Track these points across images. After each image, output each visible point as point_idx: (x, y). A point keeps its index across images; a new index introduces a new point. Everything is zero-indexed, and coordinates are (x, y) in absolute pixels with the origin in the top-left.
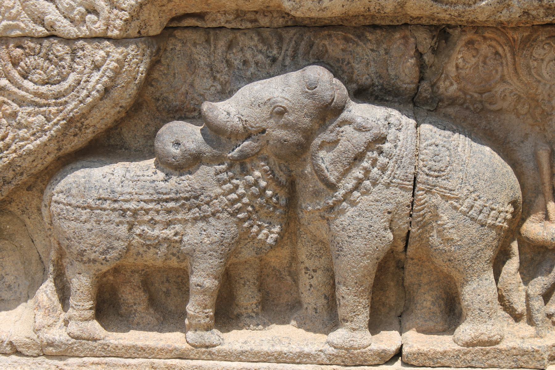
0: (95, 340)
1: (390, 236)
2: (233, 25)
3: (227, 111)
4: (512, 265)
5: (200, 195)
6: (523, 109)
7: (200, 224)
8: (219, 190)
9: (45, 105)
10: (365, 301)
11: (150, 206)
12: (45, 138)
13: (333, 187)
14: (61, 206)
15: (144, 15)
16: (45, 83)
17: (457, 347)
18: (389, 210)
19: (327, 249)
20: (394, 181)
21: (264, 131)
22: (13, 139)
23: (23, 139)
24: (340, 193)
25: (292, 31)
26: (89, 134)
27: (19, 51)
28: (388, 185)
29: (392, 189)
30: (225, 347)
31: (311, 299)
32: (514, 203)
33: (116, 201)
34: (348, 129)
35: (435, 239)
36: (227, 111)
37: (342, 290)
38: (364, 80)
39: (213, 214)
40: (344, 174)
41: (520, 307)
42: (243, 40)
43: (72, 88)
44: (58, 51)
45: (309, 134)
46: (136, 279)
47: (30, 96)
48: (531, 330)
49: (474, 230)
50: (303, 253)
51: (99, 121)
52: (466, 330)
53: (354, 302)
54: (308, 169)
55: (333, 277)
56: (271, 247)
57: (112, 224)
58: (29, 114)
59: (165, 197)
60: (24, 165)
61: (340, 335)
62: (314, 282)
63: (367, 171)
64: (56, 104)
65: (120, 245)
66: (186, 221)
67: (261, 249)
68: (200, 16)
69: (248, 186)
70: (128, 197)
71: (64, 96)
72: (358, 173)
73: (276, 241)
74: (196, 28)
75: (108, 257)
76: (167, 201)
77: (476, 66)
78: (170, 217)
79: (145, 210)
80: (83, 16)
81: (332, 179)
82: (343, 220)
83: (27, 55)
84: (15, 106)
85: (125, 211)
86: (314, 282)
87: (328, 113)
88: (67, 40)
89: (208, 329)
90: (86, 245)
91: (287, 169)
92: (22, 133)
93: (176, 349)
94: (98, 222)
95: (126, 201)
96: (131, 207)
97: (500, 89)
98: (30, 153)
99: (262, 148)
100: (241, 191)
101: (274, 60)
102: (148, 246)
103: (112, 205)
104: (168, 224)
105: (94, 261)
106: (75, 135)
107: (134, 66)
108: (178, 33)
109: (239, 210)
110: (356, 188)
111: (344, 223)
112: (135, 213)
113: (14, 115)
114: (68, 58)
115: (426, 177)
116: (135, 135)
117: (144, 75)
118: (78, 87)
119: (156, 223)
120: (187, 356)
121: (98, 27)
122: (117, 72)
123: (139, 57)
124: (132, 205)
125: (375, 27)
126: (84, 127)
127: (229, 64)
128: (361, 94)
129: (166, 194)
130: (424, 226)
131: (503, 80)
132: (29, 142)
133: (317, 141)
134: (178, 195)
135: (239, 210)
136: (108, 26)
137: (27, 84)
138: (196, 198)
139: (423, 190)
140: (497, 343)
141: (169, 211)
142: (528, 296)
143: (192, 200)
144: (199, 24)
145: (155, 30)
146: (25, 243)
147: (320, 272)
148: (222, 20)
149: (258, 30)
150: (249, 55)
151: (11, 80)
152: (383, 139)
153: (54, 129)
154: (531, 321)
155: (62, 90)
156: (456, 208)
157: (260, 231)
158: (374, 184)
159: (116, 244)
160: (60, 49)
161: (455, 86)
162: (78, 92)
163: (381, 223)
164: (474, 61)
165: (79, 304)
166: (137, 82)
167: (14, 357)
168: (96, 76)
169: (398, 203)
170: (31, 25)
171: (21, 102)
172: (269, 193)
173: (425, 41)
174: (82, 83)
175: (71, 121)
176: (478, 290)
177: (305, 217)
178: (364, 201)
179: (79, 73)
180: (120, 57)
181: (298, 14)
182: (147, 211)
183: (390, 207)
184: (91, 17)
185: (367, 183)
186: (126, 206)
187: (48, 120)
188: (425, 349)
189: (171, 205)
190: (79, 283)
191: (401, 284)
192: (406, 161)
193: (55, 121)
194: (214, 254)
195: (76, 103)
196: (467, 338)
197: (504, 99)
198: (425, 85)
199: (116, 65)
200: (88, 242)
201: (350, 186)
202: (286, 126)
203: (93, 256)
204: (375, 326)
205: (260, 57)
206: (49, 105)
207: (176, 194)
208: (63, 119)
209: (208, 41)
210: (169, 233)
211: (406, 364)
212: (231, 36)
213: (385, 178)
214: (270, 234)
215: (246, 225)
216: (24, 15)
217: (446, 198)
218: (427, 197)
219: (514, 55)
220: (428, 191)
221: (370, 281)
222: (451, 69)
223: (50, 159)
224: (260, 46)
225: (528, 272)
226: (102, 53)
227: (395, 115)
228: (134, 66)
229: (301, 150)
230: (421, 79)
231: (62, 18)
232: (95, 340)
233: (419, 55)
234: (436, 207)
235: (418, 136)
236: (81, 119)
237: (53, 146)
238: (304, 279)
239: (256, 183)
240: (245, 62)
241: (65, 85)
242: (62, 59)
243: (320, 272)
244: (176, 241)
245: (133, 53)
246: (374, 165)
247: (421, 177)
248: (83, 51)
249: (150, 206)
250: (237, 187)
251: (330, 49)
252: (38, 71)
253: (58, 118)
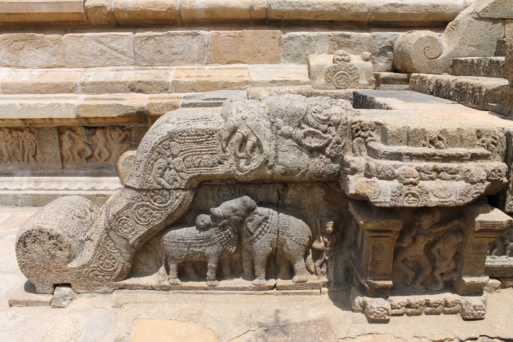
0: (178, 285)
1: (271, 249)
2: (220, 184)
3: (218, 211)
4: (310, 257)
6: (311, 207)
7: (211, 247)
8: (216, 236)
10: (264, 270)
11: (195, 241)
12: (161, 221)
13: (252, 234)
15: (192, 181)
16: (161, 203)
17: (293, 283)
19: (251, 254)
21: (230, 217)
22: (151, 221)
23: (154, 221)
24: (255, 236)
25: (238, 185)
26: (175, 219)
27: (153, 194)
28: (270, 233)
29: (271, 234)
30: (220, 286)
31: (247, 270)
32: (309, 237)
34: (256, 215)
35: (285, 249)
36: (218, 211)
37: (256, 266)
38: (261, 200)
39: (215, 243)
40: (256, 230)
41: (313, 270)
42: (223, 188)
43: (170, 205)
45: (244, 217)
46: (191, 265)
47: (156, 208)
48: (317, 277)
49: (297, 246)
50: (244, 255)
51: (178, 215)
52: (296, 278)
53: (260, 270)
54: (244, 228)
55: (253, 263)
56: (233, 253)
58: (156, 213)
61: (256, 281)
62: (247, 264)
63: (263, 228)
65: (186, 254)
66: (206, 246)
67: (230, 254)
68: (209, 181)
69: (225, 234)
72: (260, 229)
73: (235, 251)
74: (208, 185)
76: (200, 240)
77: (296, 195)
78: (201, 245)
80: (173, 182)
81: (252, 231)
82: (256, 244)
83: (156, 195)
85: (187, 243)
86: (247, 264)
87: (250, 210)
88: (168, 190)
89: (214, 280)
91: (238, 228)
92: (154, 219)
94: (178, 247)
97: (303, 201)
98: (156, 225)
99: (229, 222)
100: (223, 236)
101: (233, 194)
102: (194, 254)
104: (200, 247)
105: (177, 259)
108: (202, 187)
109: (223, 242)
110: (260, 234)
112: (190, 244)
114: (168, 195)
119: (197, 247)
121: (178, 185)
122: (183, 199)
124: (189, 241)
125: (264, 183)
127: (219, 196)
128: (261, 204)
130: (282, 245)
131: (304, 199)
133: (247, 219)
135: (223, 242)
136: (180, 185)
137: (156, 204)
138: (209, 238)
140: (306, 281)
141: (200, 243)
142: (315, 266)
143: (207, 239)
144: (209, 183)
145: (195, 186)
146: (155, 254)
147: (249, 261)
148: (216, 182)
149: (227, 185)
150: (225, 193)
151: (151, 203)
152: (268, 218)
154: (316, 274)
156: (291, 239)
158: (265, 232)
159: (184, 254)
160: (166, 193)
161: (290, 201)
163: (268, 245)
164: (295, 193)
167: (152, 291)
168: (177, 201)
169: (273, 238)
170: (157, 185)
171: (154, 209)
172: (232, 236)
173: (280, 187)
175: (169, 215)
176: (299, 265)
177: (244, 243)
178: (262, 238)
181: (240, 180)
182: (194, 243)
183: (270, 240)
185: (263, 232)
186: (187, 241)
187: (162, 215)
188: (283, 284)
189: (201, 241)
191: (275, 264)
192: (275, 225)
196: (296, 280)
197: (305, 204)
198: (280, 201)
201: (258, 233)
202: (237, 215)
203: (177, 258)
204: (267, 278)
205: (228, 193)
209: (212, 189)
210: (201, 250)
211: (277, 289)
212: (219, 187)
213: (269, 231)
214: (233, 249)
216: (155, 182)
217: (288, 236)
218: (282, 236)
219: (307, 191)
220: (282, 234)
221: (265, 263)
222: (289, 196)
223: (163, 227)
224: (228, 190)
225: (315, 259)
226: (179, 193)
227: (271, 210)
229: (241, 223)
230: (279, 199)
231: (166, 183)
232: (178, 285)
233: (278, 192)
234: (285, 239)
235: (279, 217)
237: (164, 223)
238: (244, 264)
239: (228, 233)
240: (224, 195)
241: (167, 204)
242: (166, 196)
243: (249, 261)
246: (265, 226)
247: (280, 230)
249: (195, 241)
250: (222, 235)
251: (250, 190)
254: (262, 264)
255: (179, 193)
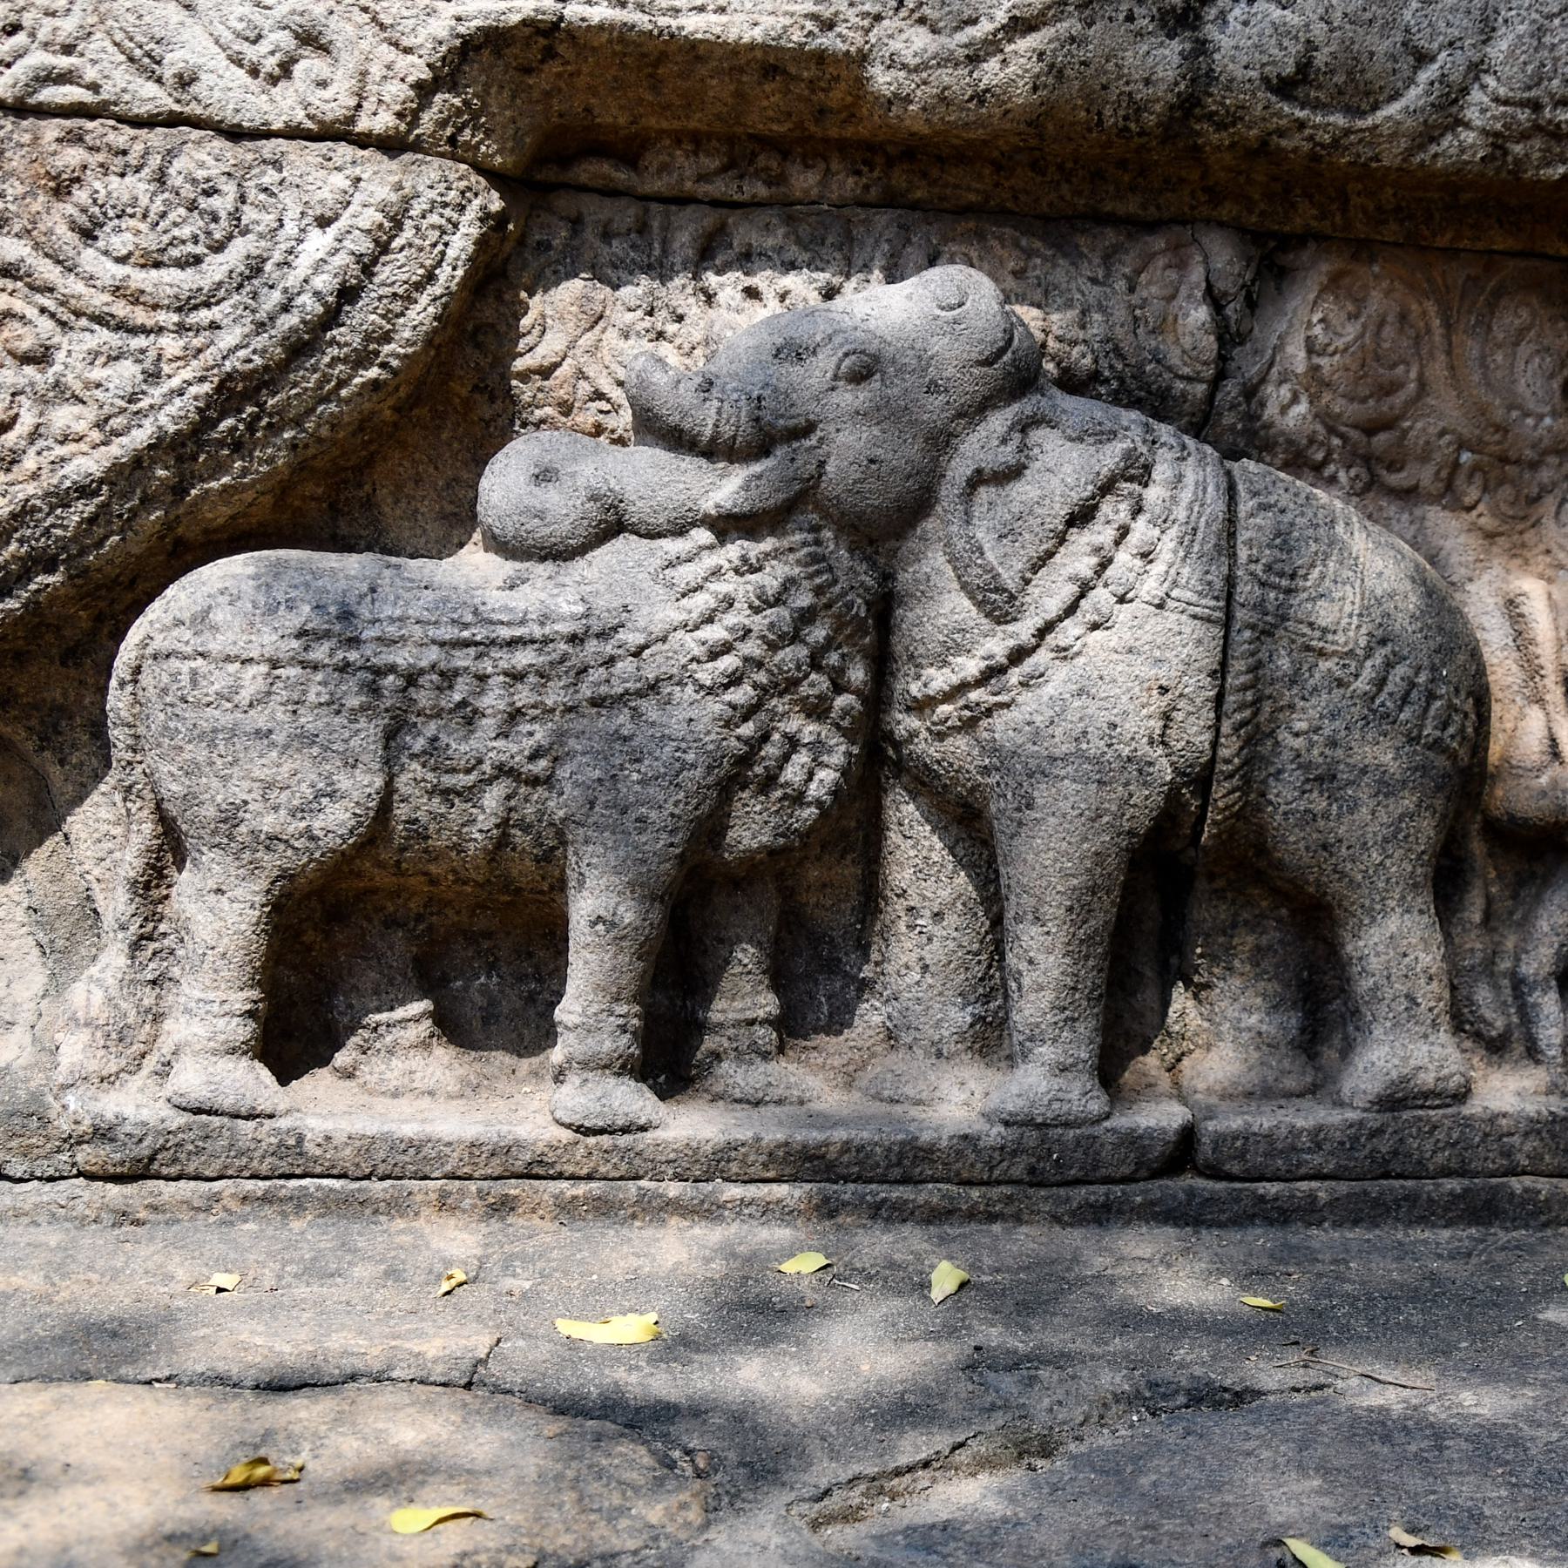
5: (615, 629)
9: (145, 330)
12: (141, 436)
14: (174, 663)
18: (1164, 682)
20: (1174, 594)
22: (35, 435)
33: (354, 642)
44: (202, 165)
57: (338, 712)
59: (505, 633)
60: (59, 532)
64: (181, 329)
70: (392, 630)
71: (207, 305)
75: (317, 824)
79: (442, 674)
83: (104, 168)
84: (46, 325)
85: (379, 672)
90: (246, 784)
93: (518, 1144)
95: (385, 641)
96: (400, 661)
103: (340, 655)
106: (238, 447)
107: (433, 235)
111: (1038, 719)
113: (40, 357)
114: (230, 189)
115: (1258, 591)
116: (416, 511)
117: (460, 272)
118: (255, 282)
120: (552, 1165)
123: (448, 212)
126: (263, 423)
129: (509, 624)
132: (83, 447)
133: (959, 469)
134: (547, 630)
139: (1253, 627)
153: (171, 410)
155: (206, 283)
157: (786, 758)
159: (344, 782)
162: (255, 295)
165: (211, 996)
166: (437, 290)
171: (70, 316)
174: (268, 267)
179: (261, 236)
180: (394, 197)
182: (449, 677)
184: (310, 65)
190: (218, 925)
193: (175, 382)
194: (653, 815)
195: (246, 330)
199: (379, 217)
200: (257, 773)
203: (269, 823)
206: (160, 330)
207: (542, 624)
208: (202, 380)
215: (747, 729)
228: (433, 235)
236: (258, 389)
241: (217, 268)
244: (534, 781)
245: (432, 194)
248: (280, 170)
252: (132, 223)
253: (186, 374)
254: (1079, 909)
255: (340, 181)
